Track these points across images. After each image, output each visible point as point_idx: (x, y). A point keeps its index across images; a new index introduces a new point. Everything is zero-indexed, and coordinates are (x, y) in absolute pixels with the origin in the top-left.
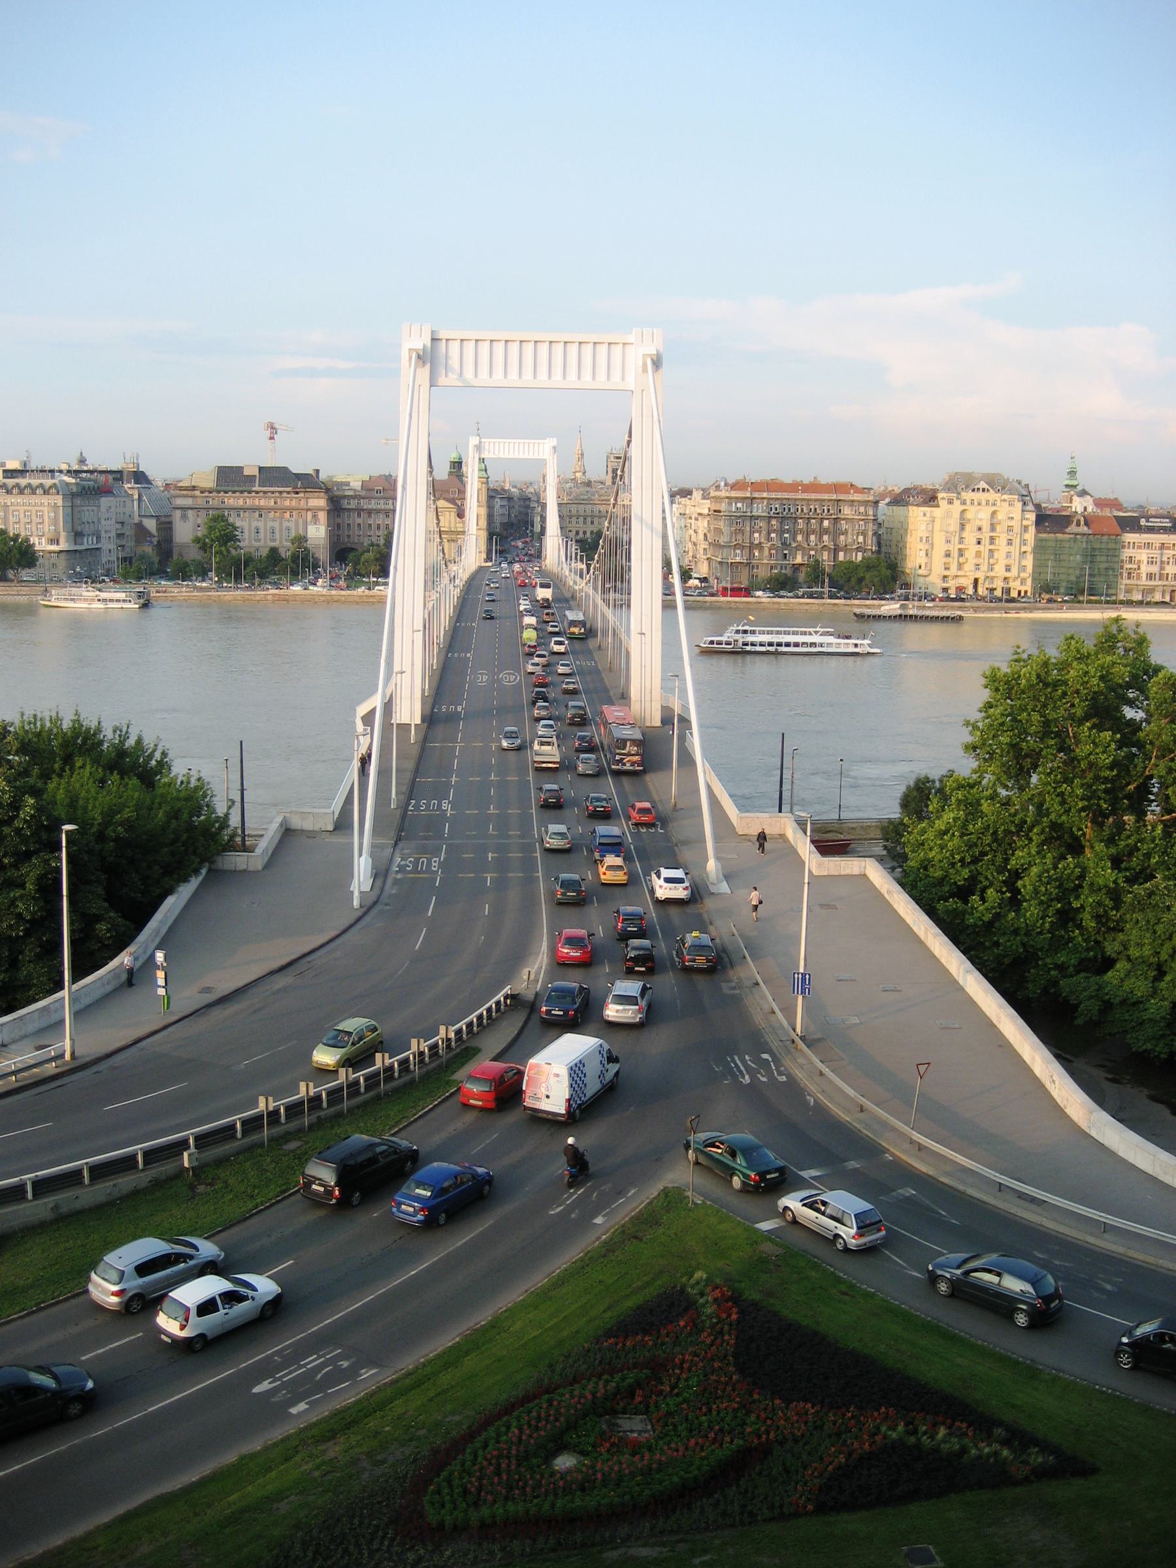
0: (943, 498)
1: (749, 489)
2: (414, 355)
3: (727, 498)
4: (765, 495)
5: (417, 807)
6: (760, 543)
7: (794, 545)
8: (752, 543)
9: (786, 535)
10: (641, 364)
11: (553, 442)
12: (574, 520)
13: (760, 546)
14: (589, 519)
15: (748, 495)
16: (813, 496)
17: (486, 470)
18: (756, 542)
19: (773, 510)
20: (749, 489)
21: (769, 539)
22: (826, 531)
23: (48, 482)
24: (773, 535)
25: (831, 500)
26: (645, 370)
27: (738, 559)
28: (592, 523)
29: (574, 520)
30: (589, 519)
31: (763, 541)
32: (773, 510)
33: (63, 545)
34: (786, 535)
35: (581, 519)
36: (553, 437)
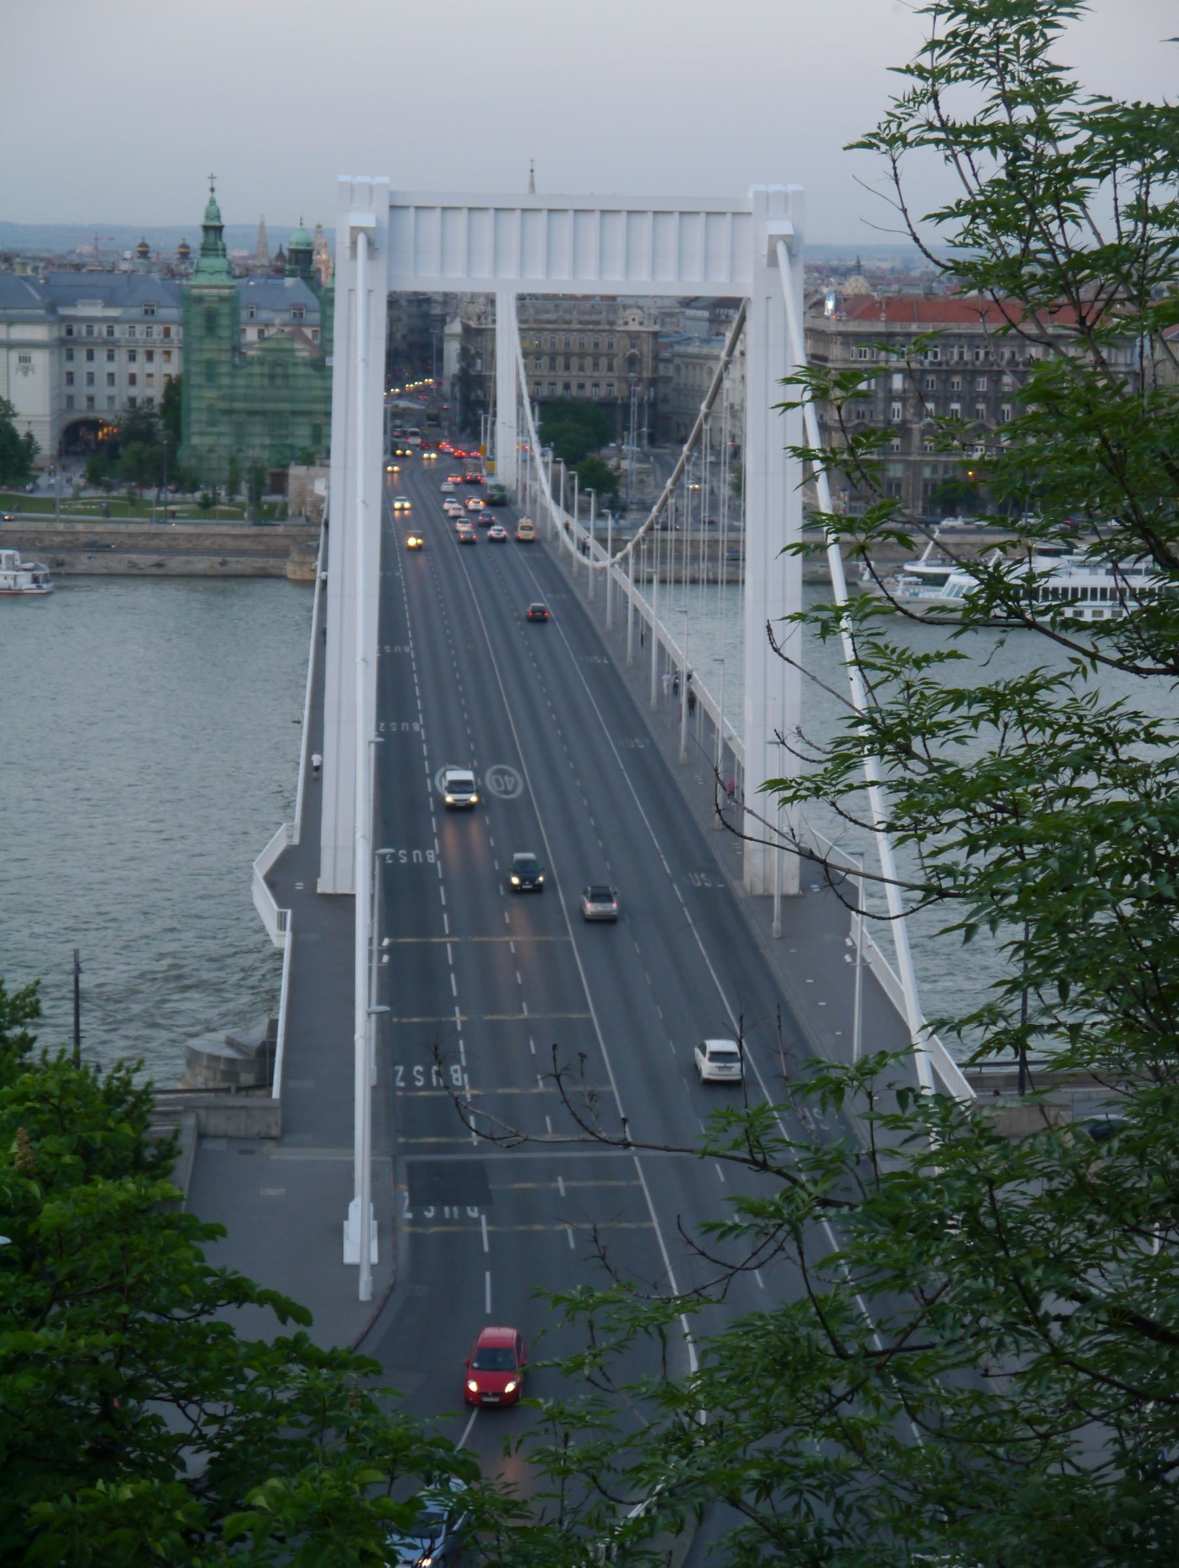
1: (883, 316)
2: (361, 240)
3: (840, 334)
5: (409, 1077)
6: (904, 422)
8: (889, 422)
9: (956, 406)
10: (765, 252)
14: (560, 361)
15: (880, 327)
18: (897, 420)
20: (883, 316)
21: (920, 413)
26: (773, 261)
30: (560, 361)
31: (909, 416)
34: (956, 406)
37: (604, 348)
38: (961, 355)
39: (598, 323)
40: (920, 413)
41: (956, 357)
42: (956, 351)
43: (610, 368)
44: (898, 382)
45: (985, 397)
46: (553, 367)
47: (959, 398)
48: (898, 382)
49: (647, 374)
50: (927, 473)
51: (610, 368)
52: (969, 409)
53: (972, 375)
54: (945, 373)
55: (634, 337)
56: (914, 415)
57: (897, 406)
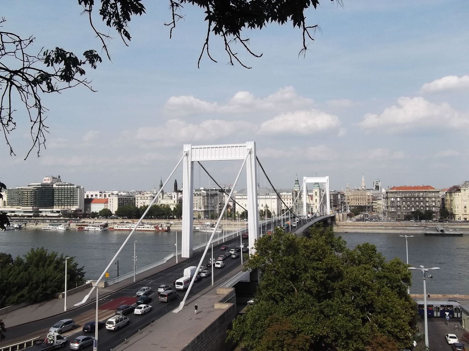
0: (462, 189)
4: (401, 191)
6: (400, 206)
7: (411, 206)
11: (327, 177)
12: (353, 200)
13: (400, 206)
14: (357, 200)
16: (417, 191)
17: (319, 187)
19: (404, 195)
22: (422, 201)
23: (199, 193)
24: (404, 203)
25: (423, 191)
27: (393, 211)
28: (358, 201)
29: (353, 200)
32: (404, 195)
33: (203, 209)
35: (355, 200)
36: (328, 176)
37: (364, 198)
38: (409, 195)
39: (363, 194)
40: (402, 204)
41: (408, 195)
42: (408, 194)
43: (365, 201)
44: (398, 199)
45: (413, 201)
46: (356, 201)
47: (409, 202)
48: (398, 199)
49: (371, 201)
50: (404, 213)
51: (365, 201)
52: (411, 203)
53: (411, 198)
54: (406, 198)
55: (369, 196)
56: (402, 204)
57: (399, 203)
